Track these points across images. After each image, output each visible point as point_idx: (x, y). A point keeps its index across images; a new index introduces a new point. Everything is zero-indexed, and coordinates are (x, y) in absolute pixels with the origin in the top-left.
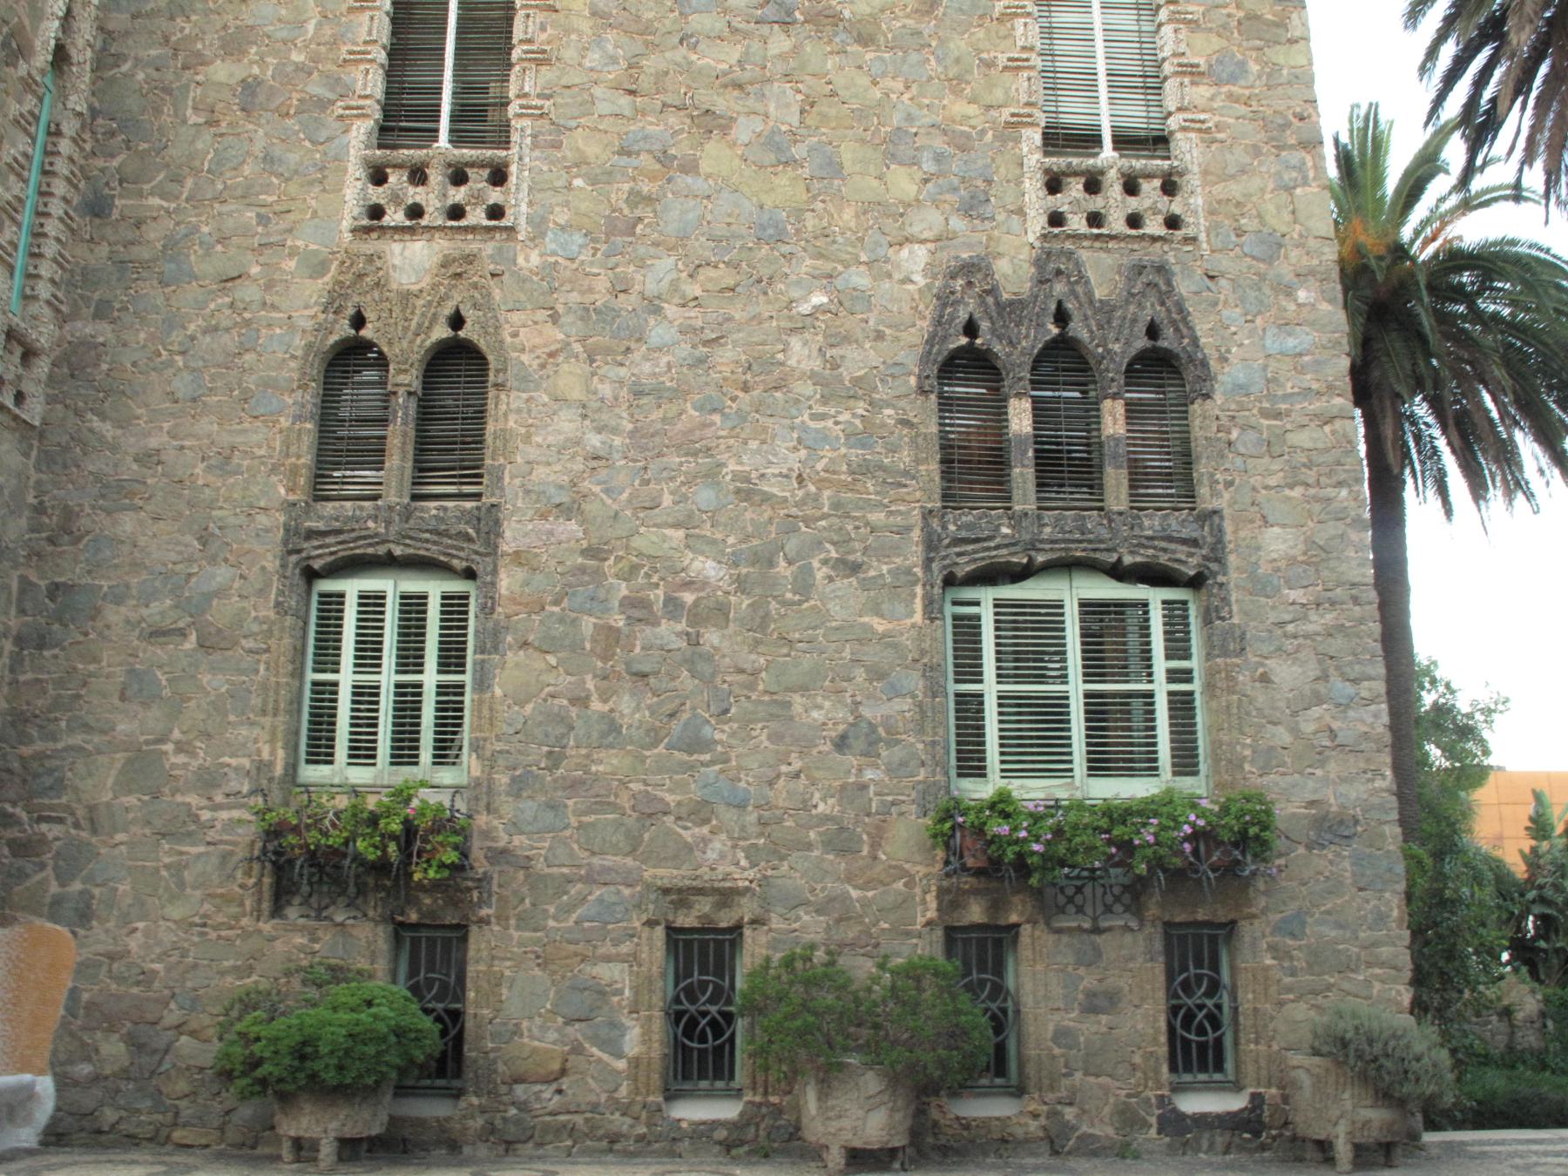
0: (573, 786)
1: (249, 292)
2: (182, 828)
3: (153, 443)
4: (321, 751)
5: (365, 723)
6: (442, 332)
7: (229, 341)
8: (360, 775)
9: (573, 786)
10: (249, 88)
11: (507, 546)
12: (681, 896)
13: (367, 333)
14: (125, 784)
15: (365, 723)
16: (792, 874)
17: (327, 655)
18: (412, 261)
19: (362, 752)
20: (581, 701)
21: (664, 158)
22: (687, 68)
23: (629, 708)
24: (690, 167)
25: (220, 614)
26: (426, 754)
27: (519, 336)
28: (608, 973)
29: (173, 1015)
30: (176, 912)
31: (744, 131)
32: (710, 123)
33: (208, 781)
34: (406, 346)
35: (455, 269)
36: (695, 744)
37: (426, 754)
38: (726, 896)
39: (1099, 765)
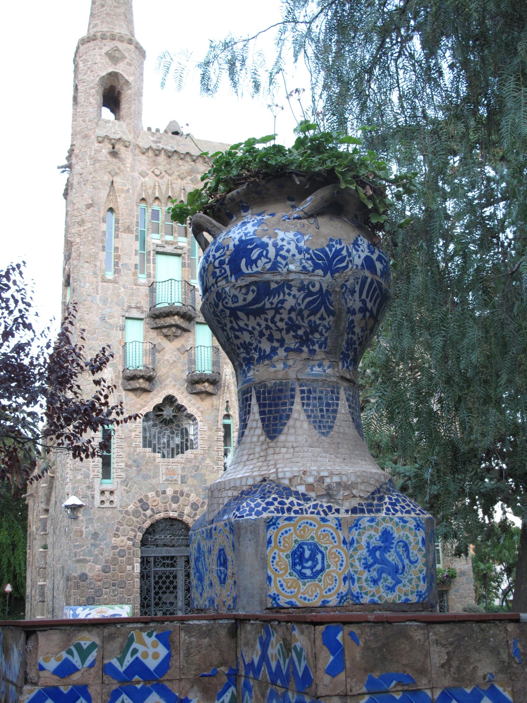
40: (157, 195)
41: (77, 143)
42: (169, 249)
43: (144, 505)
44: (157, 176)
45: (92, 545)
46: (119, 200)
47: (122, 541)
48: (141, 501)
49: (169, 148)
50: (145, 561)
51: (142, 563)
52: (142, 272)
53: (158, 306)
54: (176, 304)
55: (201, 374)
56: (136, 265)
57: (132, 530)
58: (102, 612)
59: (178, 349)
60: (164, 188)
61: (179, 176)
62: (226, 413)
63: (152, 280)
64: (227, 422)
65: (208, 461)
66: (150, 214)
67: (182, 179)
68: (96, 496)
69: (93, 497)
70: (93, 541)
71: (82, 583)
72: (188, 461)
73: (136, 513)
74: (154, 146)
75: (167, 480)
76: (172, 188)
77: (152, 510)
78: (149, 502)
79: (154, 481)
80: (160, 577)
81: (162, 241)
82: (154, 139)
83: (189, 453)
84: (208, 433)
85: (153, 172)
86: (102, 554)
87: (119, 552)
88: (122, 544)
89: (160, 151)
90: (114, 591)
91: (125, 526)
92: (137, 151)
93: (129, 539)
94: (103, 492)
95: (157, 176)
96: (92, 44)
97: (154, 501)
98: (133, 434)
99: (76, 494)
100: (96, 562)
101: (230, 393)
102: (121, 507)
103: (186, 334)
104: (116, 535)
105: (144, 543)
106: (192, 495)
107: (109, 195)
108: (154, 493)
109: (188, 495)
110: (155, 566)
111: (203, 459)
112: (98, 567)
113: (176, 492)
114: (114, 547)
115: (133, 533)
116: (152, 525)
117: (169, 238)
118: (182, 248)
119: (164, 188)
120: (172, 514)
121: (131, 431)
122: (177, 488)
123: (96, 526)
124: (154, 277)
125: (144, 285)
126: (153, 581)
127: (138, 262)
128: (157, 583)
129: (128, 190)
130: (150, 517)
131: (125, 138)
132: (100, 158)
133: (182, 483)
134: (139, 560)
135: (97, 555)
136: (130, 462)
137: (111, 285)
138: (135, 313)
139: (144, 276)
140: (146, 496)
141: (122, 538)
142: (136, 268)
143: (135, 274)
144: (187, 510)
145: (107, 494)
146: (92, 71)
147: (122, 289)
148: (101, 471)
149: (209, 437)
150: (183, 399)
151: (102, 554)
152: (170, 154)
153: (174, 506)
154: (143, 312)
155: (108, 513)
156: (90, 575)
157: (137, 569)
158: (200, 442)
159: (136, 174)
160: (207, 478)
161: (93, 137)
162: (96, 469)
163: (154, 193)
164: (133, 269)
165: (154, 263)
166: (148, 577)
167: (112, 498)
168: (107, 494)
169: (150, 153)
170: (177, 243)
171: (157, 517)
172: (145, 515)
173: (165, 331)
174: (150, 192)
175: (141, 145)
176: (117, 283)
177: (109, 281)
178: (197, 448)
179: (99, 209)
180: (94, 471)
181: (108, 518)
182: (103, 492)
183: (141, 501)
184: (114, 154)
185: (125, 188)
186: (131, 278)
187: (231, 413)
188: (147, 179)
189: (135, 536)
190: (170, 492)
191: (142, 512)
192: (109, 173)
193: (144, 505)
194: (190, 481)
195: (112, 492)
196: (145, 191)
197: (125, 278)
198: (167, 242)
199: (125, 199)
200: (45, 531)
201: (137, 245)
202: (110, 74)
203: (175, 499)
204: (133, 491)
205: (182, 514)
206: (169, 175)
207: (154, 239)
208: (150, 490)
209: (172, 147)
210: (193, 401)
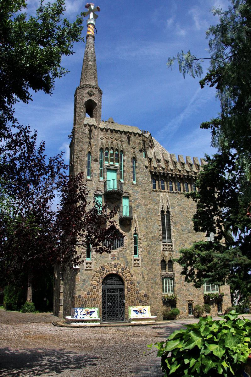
0: (181, 294)
1: (155, 255)
2: (156, 298)
3: (150, 268)
4: (163, 292)
5: (166, 289)
6: (169, 259)
7: (155, 259)
8: (166, 293)
9: (181, 294)
10: (153, 237)
12: (189, 301)
13: (164, 259)
14: (152, 295)
15: (166, 289)
16: (195, 299)
17: (163, 284)
18: (167, 253)
19: (166, 291)
20: (181, 287)
21: (183, 244)
22: (183, 236)
23: (184, 287)
24: (185, 245)
25: (157, 281)
26: (170, 291)
28: (184, 306)
29: (157, 311)
30: (157, 304)
31: (188, 242)
32: (186, 241)
33: (158, 294)
34: (167, 260)
36: (188, 290)
37: (170, 291)
38: (191, 301)
39: (212, 291)
40: (107, 146)
41: (76, 126)
42: (112, 167)
43: (103, 268)
45: (83, 284)
46: (92, 148)
47: (95, 283)
48: (102, 267)
49: (111, 128)
50: (103, 291)
51: (102, 291)
52: (101, 176)
53: (108, 190)
54: (115, 189)
55: (125, 217)
56: (99, 174)
57: (98, 278)
58: (87, 310)
60: (110, 144)
61: (115, 139)
62: (134, 232)
63: (105, 179)
64: (135, 235)
65: (128, 251)
66: (104, 154)
67: (117, 140)
68: (84, 265)
70: (83, 283)
71: (79, 299)
73: (100, 272)
74: (106, 128)
75: (112, 259)
77: (106, 270)
79: (107, 259)
80: (109, 297)
81: (109, 164)
82: (106, 125)
83: (121, 248)
84: (128, 240)
85: (105, 138)
86: (87, 288)
87: (93, 287)
88: (95, 284)
89: (108, 129)
90: (92, 302)
91: (96, 277)
92: (99, 129)
93: (97, 282)
94: (87, 264)
95: (107, 139)
96: (82, 89)
97: (107, 267)
100: (84, 291)
101: (136, 224)
102: (94, 269)
103: (119, 201)
104: (92, 281)
105: (103, 283)
106: (122, 264)
108: (107, 264)
109: (120, 265)
110: (107, 293)
111: (126, 251)
112: (86, 293)
113: (115, 264)
114: (91, 285)
115: (99, 280)
117: (112, 163)
118: (117, 167)
119: (110, 144)
120: (114, 272)
122: (116, 262)
123: (85, 277)
124: (106, 179)
125: (102, 182)
126: (107, 298)
127: (100, 172)
128: (108, 299)
129: (96, 144)
131: (94, 124)
132: (85, 132)
133: (118, 260)
134: (101, 290)
135: (85, 288)
137: (89, 182)
139: (102, 178)
142: (99, 175)
143: (99, 177)
144: (120, 270)
145: (89, 264)
146: (82, 99)
147: (94, 183)
148: (86, 255)
149: (128, 241)
151: (87, 288)
152: (112, 131)
153: (115, 269)
154: (102, 192)
156: (83, 296)
157: (101, 293)
158: (124, 244)
159: (99, 138)
160: (128, 258)
161: (83, 124)
163: (106, 146)
164: (98, 175)
165: (106, 173)
166: (105, 297)
167: (90, 266)
169: (104, 130)
170: (115, 165)
171: (108, 273)
172: (103, 273)
174: (104, 145)
175: (100, 127)
176: (92, 181)
177: (89, 180)
178: (123, 246)
179: (85, 152)
182: (87, 264)
183: (102, 267)
184: (90, 131)
185: (95, 144)
186: (97, 179)
187: (137, 232)
188: (103, 140)
190: (113, 263)
193: (103, 268)
194: (121, 259)
195: (90, 264)
197: (95, 179)
198: (111, 165)
199: (95, 148)
201: (100, 166)
202: (89, 100)
203: (115, 266)
205: (118, 272)
206: (112, 139)
207: (106, 163)
208: (105, 262)
209: (113, 128)
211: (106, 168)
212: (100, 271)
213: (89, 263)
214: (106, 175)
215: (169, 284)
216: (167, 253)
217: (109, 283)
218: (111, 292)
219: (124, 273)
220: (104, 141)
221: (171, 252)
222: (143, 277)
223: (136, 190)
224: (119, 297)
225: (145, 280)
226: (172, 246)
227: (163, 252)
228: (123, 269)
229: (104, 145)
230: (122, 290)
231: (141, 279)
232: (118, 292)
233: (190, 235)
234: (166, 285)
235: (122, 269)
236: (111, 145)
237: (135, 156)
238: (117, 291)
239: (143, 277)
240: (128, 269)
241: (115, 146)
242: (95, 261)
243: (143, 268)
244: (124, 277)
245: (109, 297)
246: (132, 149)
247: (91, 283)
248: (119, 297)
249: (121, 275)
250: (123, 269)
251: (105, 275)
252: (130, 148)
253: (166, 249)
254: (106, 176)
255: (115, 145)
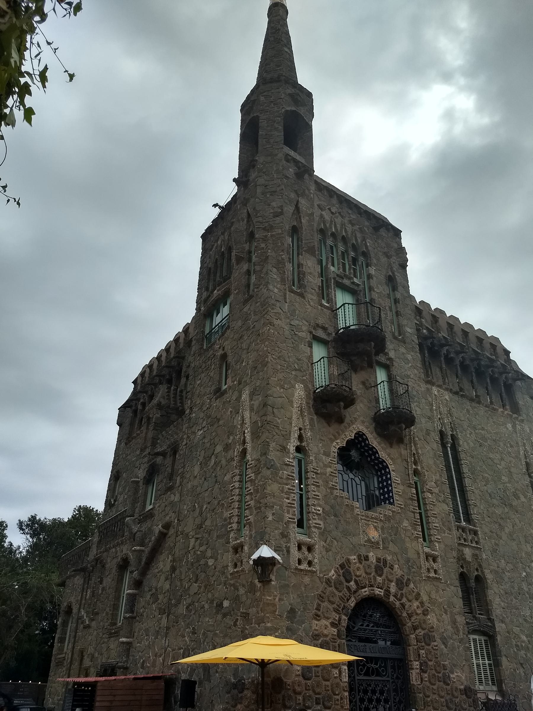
6: (476, 573)
11: (497, 630)
13: (465, 570)
27: (489, 576)
31: (507, 530)
35: (475, 556)
44: (332, 213)
46: (302, 221)
48: (342, 566)
57: (336, 611)
59: (363, 383)
69: (288, 552)
72: (388, 519)
76: (345, 229)
78: (351, 569)
79: (354, 540)
84: (401, 487)
85: (329, 209)
88: (325, 632)
91: (326, 604)
93: (333, 625)
97: (358, 569)
98: (329, 470)
99: (268, 543)
104: (317, 617)
107: (293, 214)
113: (378, 560)
116: (357, 604)
121: (326, 466)
122: (380, 554)
130: (355, 592)
132: (288, 175)
133: (384, 548)
136: (327, 508)
138: (320, 333)
140: (348, 560)
141: (324, 622)
145: (304, 549)
150: (374, 441)
153: (379, 579)
155: (307, 580)
158: (396, 497)
162: (291, 510)
168: (304, 549)
172: (349, 588)
173: (353, 358)
180: (288, 513)
181: (305, 586)
189: (340, 620)
191: (346, 584)
192: (296, 192)
196: (324, 223)
200: (132, 612)
203: (379, 570)
204: (334, 550)
205: (388, 592)
210: (383, 445)
211: (334, 278)
212: (341, 583)
213: (304, 544)
214: (335, 295)
215: (483, 659)
216: (468, 552)
217: (361, 634)
218: (367, 674)
219: (404, 600)
220: (327, 216)
221: (477, 552)
222: (454, 622)
223: (403, 354)
224: (392, 694)
225: (458, 631)
226: (475, 533)
227: (461, 548)
228: (401, 584)
229: (328, 225)
230: (402, 665)
231: (449, 627)
232: (390, 670)
233: (506, 510)
234: (477, 658)
235: (397, 584)
236: (341, 230)
237: (393, 273)
238: (385, 667)
239: (454, 622)
240: (412, 585)
241: (349, 236)
242: (322, 543)
243: (448, 585)
244: (405, 614)
245: (365, 692)
246: (386, 259)
247: (314, 627)
248: (392, 694)
249: (398, 603)
250: (401, 584)
251: (352, 603)
252: (381, 254)
253: (465, 540)
254: (335, 298)
255: (349, 233)
